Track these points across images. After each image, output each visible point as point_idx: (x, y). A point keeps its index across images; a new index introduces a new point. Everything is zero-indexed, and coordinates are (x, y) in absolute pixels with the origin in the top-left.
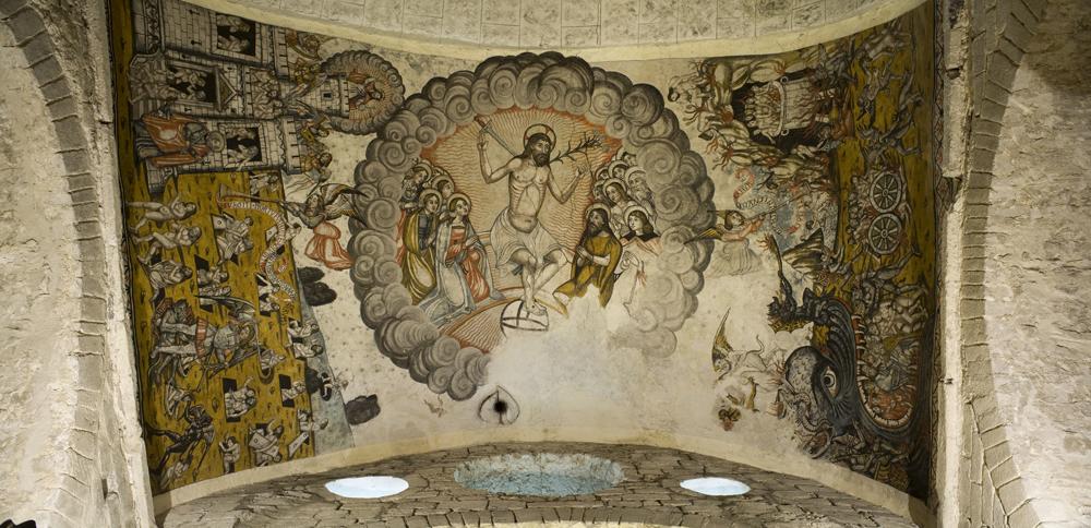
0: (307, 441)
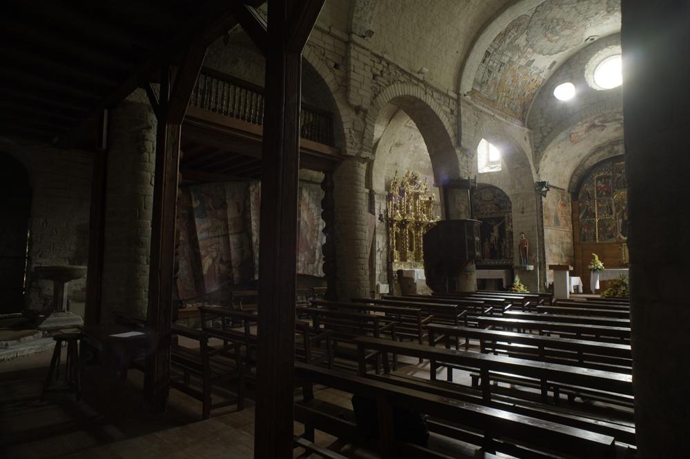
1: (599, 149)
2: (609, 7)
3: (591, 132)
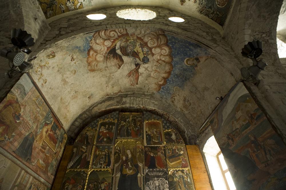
0: (81, 5)
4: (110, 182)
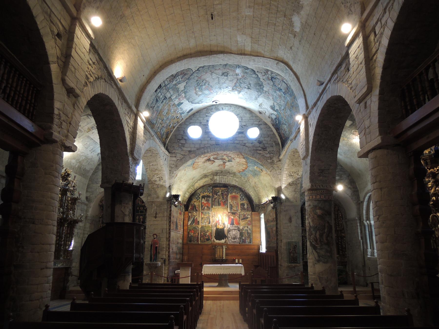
1: (205, 176)
2: (235, 86)
3: (205, 164)
4: (211, 232)
